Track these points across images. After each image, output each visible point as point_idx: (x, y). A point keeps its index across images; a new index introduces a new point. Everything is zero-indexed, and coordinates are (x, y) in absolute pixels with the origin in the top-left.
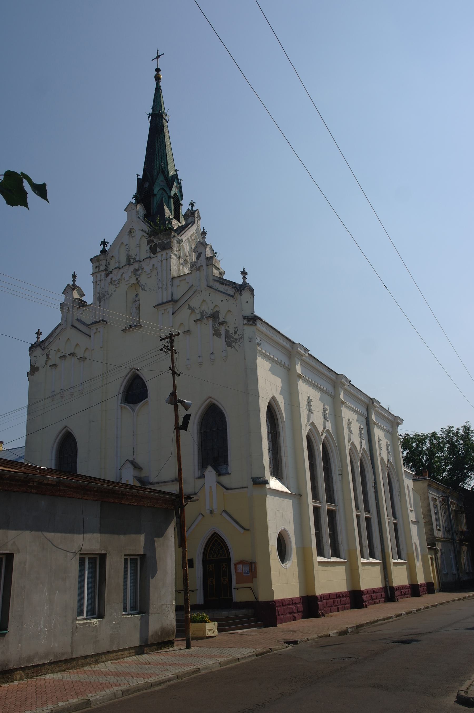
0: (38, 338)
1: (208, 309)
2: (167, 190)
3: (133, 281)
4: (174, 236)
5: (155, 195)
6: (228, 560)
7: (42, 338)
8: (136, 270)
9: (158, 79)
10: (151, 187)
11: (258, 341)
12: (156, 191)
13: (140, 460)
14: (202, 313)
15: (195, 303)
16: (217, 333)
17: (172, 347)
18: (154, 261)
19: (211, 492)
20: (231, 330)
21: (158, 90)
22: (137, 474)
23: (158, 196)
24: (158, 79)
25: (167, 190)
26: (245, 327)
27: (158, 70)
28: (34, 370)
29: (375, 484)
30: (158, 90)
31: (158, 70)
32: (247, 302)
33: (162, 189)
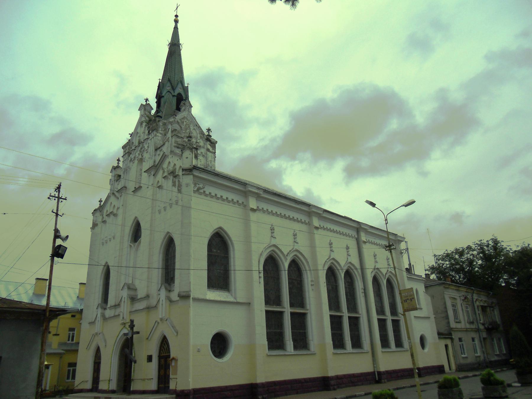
0: (100, 204)
1: (171, 168)
2: (172, 92)
3: (140, 157)
4: (159, 121)
5: (163, 96)
6: (169, 356)
7: (102, 203)
8: (141, 148)
9: (176, 21)
10: (161, 93)
11: (201, 186)
12: (163, 95)
13: (137, 284)
14: (168, 171)
15: (165, 165)
16: (174, 185)
17: (59, 195)
18: (149, 141)
19: (162, 304)
20: (181, 180)
21: (176, 28)
22: (132, 293)
23: (165, 97)
24: (176, 21)
25: (172, 92)
26: (184, 177)
27: (176, 16)
28: (95, 225)
29: (365, 289)
30: (176, 28)
31: (176, 16)
32: (187, 158)
33: (168, 91)
